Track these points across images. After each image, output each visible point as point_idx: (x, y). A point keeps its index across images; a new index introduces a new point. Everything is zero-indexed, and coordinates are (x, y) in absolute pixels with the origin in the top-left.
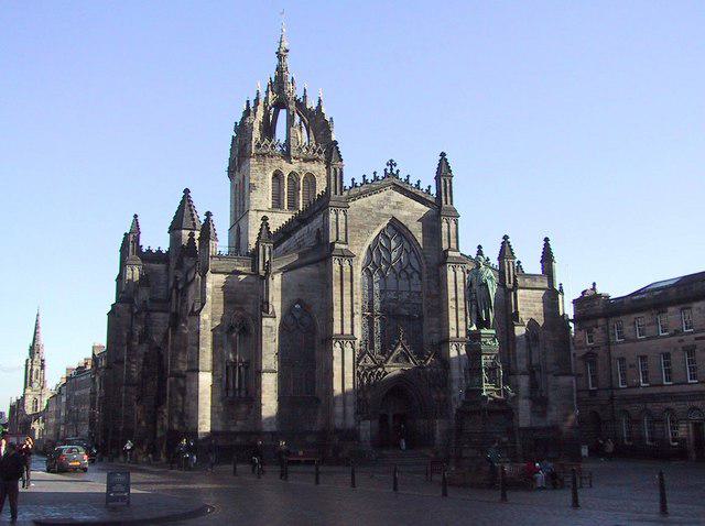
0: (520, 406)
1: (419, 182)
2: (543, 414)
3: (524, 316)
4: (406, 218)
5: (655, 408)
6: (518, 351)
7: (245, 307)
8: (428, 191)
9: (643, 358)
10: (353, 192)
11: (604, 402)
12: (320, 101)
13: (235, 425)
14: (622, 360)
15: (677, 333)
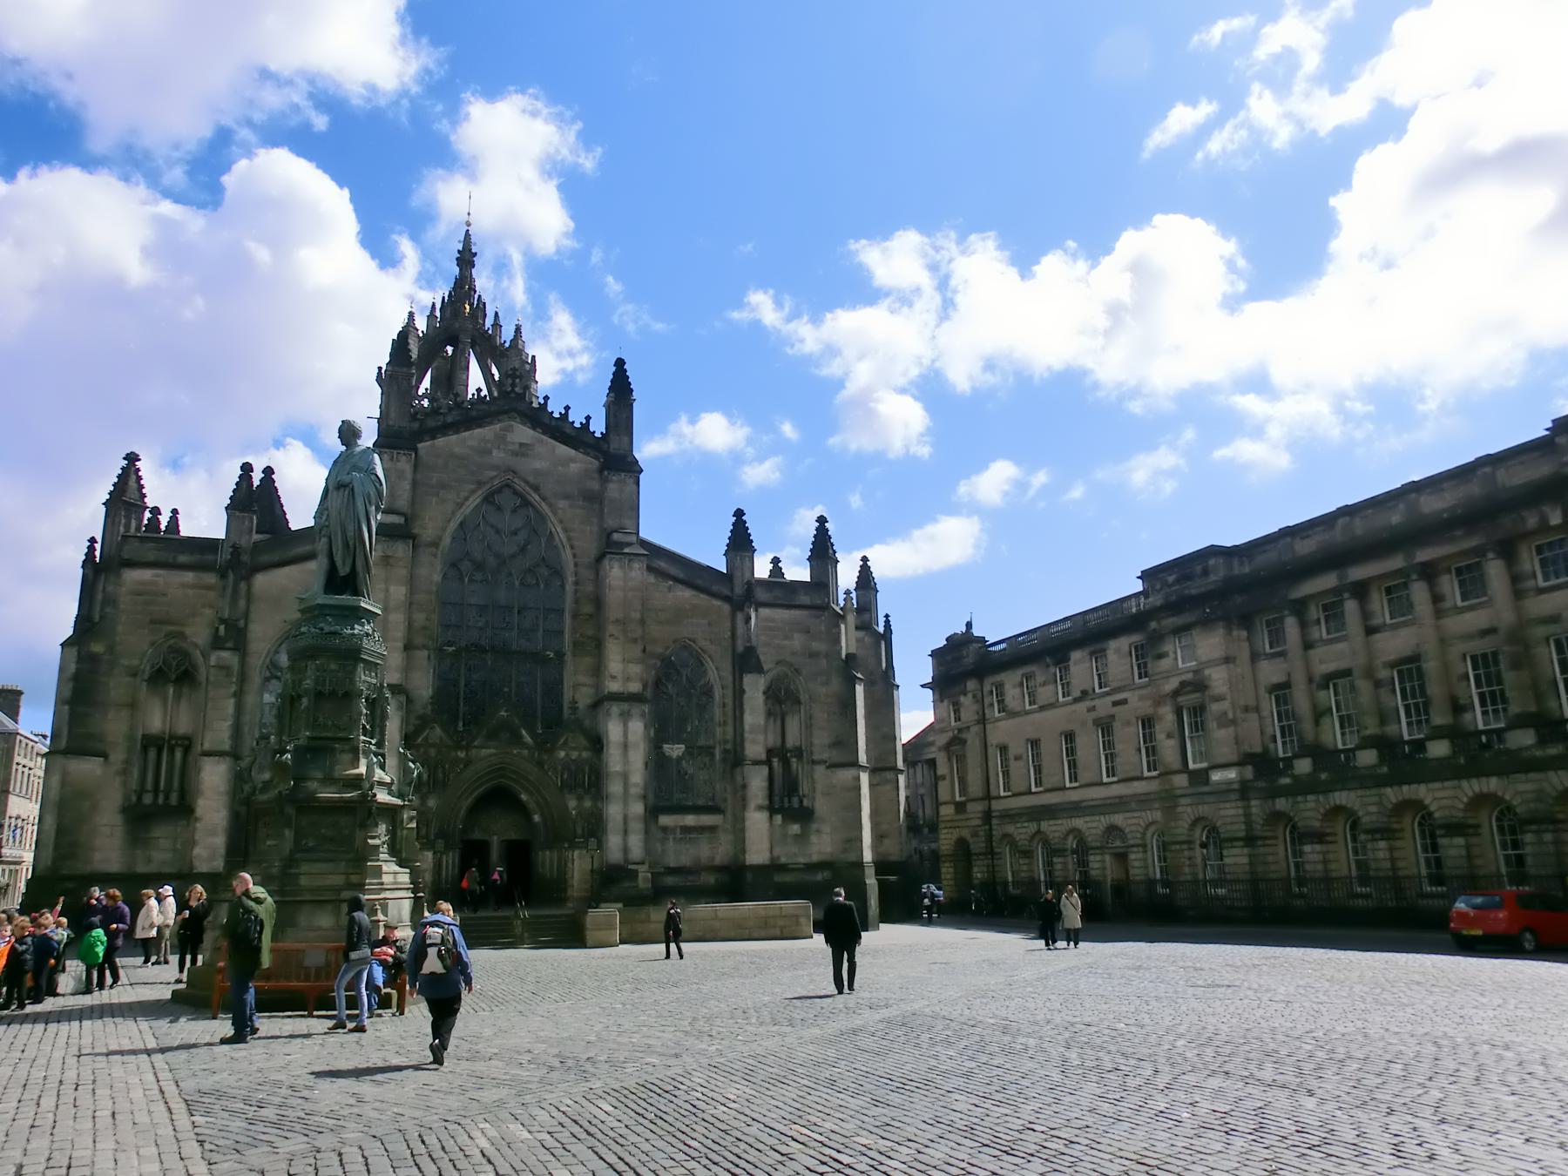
0: (748, 823)
1: (567, 408)
2: (802, 838)
3: (767, 658)
4: (537, 472)
5: (1054, 829)
6: (748, 719)
7: (188, 631)
8: (585, 426)
9: (1035, 743)
10: (431, 423)
11: (978, 822)
12: (518, 330)
13: (149, 860)
14: (1003, 749)
15: (1084, 693)
